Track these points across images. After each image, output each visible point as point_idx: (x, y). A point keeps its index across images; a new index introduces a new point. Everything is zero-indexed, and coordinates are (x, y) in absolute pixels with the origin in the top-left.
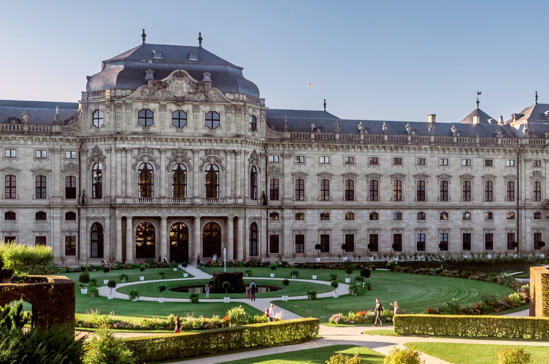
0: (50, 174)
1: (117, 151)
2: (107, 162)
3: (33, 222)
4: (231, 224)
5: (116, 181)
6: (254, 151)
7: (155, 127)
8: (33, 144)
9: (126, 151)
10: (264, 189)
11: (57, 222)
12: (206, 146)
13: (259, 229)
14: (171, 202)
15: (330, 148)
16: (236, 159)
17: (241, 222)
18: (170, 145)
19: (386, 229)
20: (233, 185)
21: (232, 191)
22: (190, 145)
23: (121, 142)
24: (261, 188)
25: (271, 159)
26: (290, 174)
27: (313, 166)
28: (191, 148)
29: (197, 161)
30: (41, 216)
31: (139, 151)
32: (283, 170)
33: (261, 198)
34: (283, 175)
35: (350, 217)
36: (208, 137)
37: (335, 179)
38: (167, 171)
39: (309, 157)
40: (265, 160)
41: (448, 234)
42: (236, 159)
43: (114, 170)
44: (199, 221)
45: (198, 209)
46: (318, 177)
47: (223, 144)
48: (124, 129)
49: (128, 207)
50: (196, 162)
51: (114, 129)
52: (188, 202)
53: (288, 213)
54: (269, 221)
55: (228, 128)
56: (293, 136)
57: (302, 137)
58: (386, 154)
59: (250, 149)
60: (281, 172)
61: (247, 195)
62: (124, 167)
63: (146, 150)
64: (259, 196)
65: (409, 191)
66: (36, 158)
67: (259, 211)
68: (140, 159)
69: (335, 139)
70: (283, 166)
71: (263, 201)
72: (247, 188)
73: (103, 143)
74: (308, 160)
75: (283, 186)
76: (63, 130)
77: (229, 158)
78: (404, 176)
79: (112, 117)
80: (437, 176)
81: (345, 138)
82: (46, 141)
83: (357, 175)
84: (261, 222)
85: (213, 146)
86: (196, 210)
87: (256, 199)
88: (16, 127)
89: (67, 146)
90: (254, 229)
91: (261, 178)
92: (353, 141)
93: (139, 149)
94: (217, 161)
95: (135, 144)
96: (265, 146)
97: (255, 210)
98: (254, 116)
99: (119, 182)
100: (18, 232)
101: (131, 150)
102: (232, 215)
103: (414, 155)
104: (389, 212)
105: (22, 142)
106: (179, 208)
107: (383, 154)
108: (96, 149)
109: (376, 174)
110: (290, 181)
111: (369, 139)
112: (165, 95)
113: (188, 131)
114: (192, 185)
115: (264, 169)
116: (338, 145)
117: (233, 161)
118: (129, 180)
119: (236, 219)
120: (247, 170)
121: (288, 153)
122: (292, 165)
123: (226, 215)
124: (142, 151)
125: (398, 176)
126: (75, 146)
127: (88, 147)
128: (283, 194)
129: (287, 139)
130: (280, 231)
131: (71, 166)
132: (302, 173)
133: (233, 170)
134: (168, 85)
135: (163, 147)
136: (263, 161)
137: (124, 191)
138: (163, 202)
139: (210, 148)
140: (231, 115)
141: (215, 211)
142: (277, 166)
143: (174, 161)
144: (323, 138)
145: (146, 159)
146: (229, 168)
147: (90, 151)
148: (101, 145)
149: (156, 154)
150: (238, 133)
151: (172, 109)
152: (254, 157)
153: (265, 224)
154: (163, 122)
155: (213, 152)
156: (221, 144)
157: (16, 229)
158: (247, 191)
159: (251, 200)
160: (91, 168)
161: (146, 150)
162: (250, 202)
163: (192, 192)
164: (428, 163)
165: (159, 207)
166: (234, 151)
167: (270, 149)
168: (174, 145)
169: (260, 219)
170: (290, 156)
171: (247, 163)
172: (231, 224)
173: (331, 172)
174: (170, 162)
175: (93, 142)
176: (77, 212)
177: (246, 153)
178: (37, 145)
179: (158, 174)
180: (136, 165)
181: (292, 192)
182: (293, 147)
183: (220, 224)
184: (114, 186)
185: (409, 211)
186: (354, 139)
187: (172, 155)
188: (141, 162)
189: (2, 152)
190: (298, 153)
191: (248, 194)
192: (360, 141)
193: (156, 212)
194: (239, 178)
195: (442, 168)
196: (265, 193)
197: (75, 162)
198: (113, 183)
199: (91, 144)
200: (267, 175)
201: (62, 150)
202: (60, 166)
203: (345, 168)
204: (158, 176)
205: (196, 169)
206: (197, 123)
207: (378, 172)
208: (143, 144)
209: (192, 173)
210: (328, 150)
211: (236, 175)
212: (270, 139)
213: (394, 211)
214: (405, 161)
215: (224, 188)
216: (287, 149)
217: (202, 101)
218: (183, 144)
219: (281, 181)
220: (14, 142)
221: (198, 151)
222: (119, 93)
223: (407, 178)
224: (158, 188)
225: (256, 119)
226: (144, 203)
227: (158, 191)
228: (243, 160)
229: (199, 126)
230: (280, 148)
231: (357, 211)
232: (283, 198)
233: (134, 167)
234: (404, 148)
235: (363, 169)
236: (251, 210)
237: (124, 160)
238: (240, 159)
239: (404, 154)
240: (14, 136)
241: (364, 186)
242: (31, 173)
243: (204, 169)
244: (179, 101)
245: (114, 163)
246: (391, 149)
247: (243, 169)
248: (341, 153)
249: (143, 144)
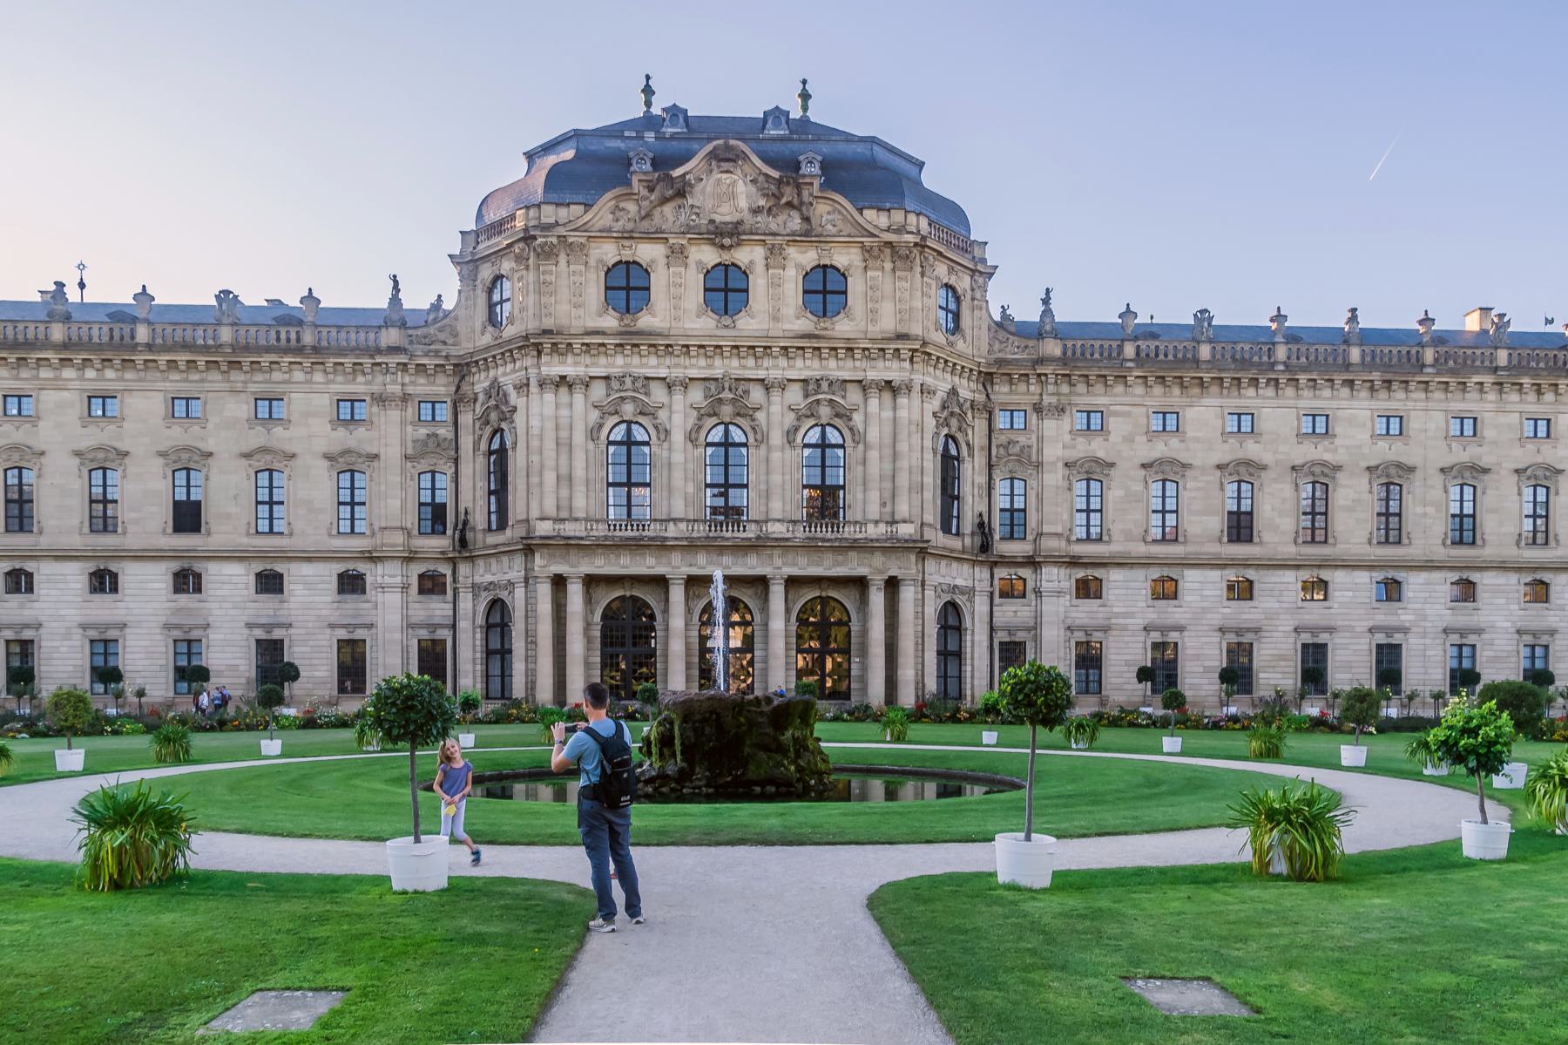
0: (376, 464)
1: (542, 385)
2: (519, 418)
3: (329, 599)
4: (877, 599)
5: (541, 474)
6: (953, 392)
7: (654, 316)
8: (328, 382)
9: (570, 386)
10: (985, 510)
11: (395, 598)
12: (805, 368)
13: (968, 623)
14: (701, 530)
15: (1182, 386)
16: (895, 409)
17: (908, 594)
18: (697, 367)
19: (1350, 629)
20: (887, 485)
21: (884, 504)
22: (757, 367)
23: (556, 358)
24: (971, 505)
25: (1001, 421)
26: (1060, 464)
27: (1129, 439)
28: (761, 374)
29: (777, 413)
30: (351, 584)
31: (609, 387)
32: (1040, 451)
33: (973, 534)
34: (1039, 466)
35: (1242, 591)
36: (809, 343)
37: (1195, 478)
38: (689, 445)
39: (1117, 414)
40: (985, 423)
41: (1546, 647)
42: (895, 409)
43: (535, 443)
44: (782, 588)
45: (776, 552)
46: (1143, 472)
47: (858, 364)
48: (564, 322)
49: (568, 545)
50: (776, 418)
51: (537, 324)
52: (751, 532)
53: (1054, 578)
54: (997, 600)
55: (873, 315)
56: (1069, 353)
57: (1097, 356)
58: (1355, 403)
59: (942, 382)
60: (1034, 458)
61: (929, 518)
62: (564, 434)
63: (628, 381)
64: (968, 526)
65: (1425, 515)
66: (338, 422)
67: (966, 567)
68: (612, 409)
69: (1196, 362)
70: (1040, 439)
71: (978, 540)
72: (928, 495)
73: (510, 367)
74: (1113, 423)
75: (1040, 498)
76: (411, 342)
77: (873, 403)
78: (1412, 469)
79: (531, 287)
80: (1517, 471)
81: (1228, 356)
82: (364, 374)
83: (1264, 468)
84: (971, 600)
85: (826, 368)
86: (771, 556)
87: (958, 534)
88: (283, 336)
89: (421, 387)
90: (952, 621)
91: (972, 473)
92: (1252, 364)
93: (607, 378)
94: (837, 415)
95: (594, 365)
96: (987, 379)
97: (955, 565)
98: (953, 289)
99: (550, 478)
100: (290, 625)
101: (587, 383)
102: (881, 572)
103: (1444, 406)
104: (1363, 577)
105: (298, 375)
106: (721, 550)
107: (1344, 404)
108: (496, 390)
109: (1323, 464)
110: (1060, 483)
111: (1303, 359)
112: (682, 219)
113: (750, 324)
114: (763, 487)
115: (982, 449)
116: (1206, 376)
117: (888, 414)
118: (579, 472)
119: (892, 585)
120: (928, 443)
121: (1054, 400)
122: (1067, 437)
123: (861, 571)
124: (615, 385)
125: (1393, 471)
126: (442, 387)
127: (478, 388)
128: (1041, 523)
129: (1052, 360)
130: (1028, 630)
131: (432, 445)
132: (1097, 461)
133: (888, 441)
134: (691, 186)
135: (678, 373)
136: (980, 425)
137: (564, 503)
138: (672, 531)
139: (817, 374)
140: (882, 275)
141: (828, 558)
142: (1022, 439)
143: (710, 415)
144: (1161, 357)
145: (628, 410)
146: (873, 435)
147: (481, 397)
148: (505, 374)
149: (658, 394)
150: (903, 330)
151: (705, 260)
152: (952, 409)
153: (986, 608)
154: (677, 301)
155: (825, 385)
156: (850, 363)
157: (283, 620)
158: (929, 506)
159: (940, 534)
160: (484, 446)
161: (628, 381)
162: (937, 538)
163: (763, 509)
164: (1488, 433)
165: (661, 546)
166: (889, 383)
167: (1001, 391)
168: (710, 367)
169: (970, 592)
170: (1061, 410)
171: (930, 423)
172: (877, 599)
173: (1183, 457)
174: (699, 419)
175: (487, 369)
176: (449, 573)
177: (925, 391)
178: (342, 387)
179: (665, 454)
180: (601, 426)
181: (1065, 516)
182: (1071, 385)
183: (847, 598)
184: (535, 490)
185: (1423, 576)
186: (1256, 359)
187: (706, 397)
188: (616, 419)
189: (245, 407)
190: (1085, 397)
191: (932, 515)
192: (1274, 364)
193: (650, 561)
194: (904, 464)
195: (1530, 447)
196: (986, 519)
197: (445, 432)
198: (534, 480)
199: (483, 375)
200: (990, 467)
201: (405, 398)
202: (403, 443)
203: (1226, 447)
204: (665, 461)
205: (777, 438)
206: (776, 301)
207: (1327, 457)
208: (617, 364)
209: (763, 450)
210: (1176, 391)
211: (895, 456)
212: (1000, 362)
213: (1379, 575)
214: (1415, 424)
215: (860, 496)
216: (1051, 388)
217: (793, 234)
218: (735, 362)
219: (1032, 483)
220: (277, 376)
221: (783, 385)
222: (549, 214)
223: (1418, 475)
224: (665, 494)
225: (958, 300)
226: (618, 533)
227: (665, 503)
228: (918, 413)
229: (784, 311)
230: (1032, 388)
231: (1262, 572)
232: (1040, 535)
233: (593, 433)
234: (1412, 386)
235: (1283, 448)
236: (944, 563)
237: (564, 412)
238: (909, 408)
239: (1410, 404)
240: (274, 357)
241: (1284, 500)
242: (326, 463)
243: (799, 440)
244: (726, 234)
245: (535, 422)
246: (1372, 389)
247: (916, 438)
248: (1218, 402)
249: (617, 364)
